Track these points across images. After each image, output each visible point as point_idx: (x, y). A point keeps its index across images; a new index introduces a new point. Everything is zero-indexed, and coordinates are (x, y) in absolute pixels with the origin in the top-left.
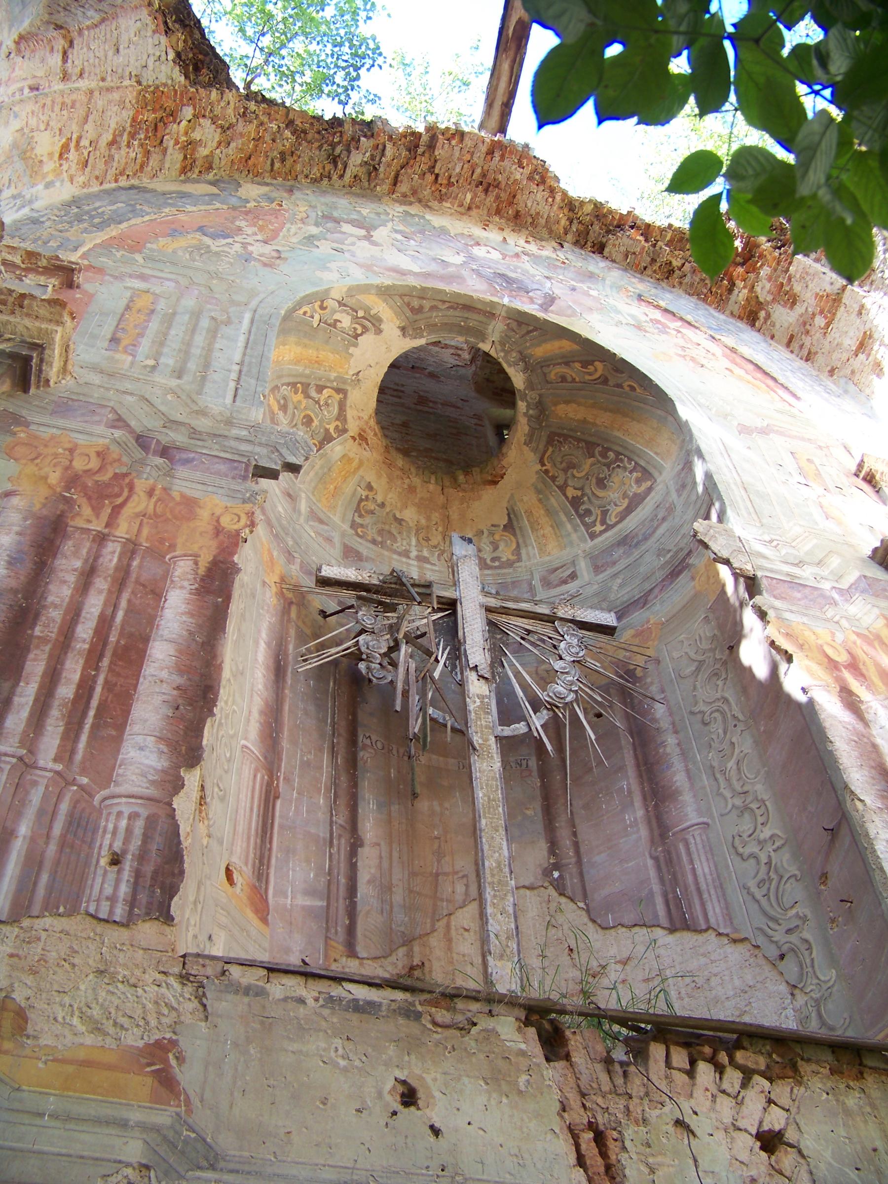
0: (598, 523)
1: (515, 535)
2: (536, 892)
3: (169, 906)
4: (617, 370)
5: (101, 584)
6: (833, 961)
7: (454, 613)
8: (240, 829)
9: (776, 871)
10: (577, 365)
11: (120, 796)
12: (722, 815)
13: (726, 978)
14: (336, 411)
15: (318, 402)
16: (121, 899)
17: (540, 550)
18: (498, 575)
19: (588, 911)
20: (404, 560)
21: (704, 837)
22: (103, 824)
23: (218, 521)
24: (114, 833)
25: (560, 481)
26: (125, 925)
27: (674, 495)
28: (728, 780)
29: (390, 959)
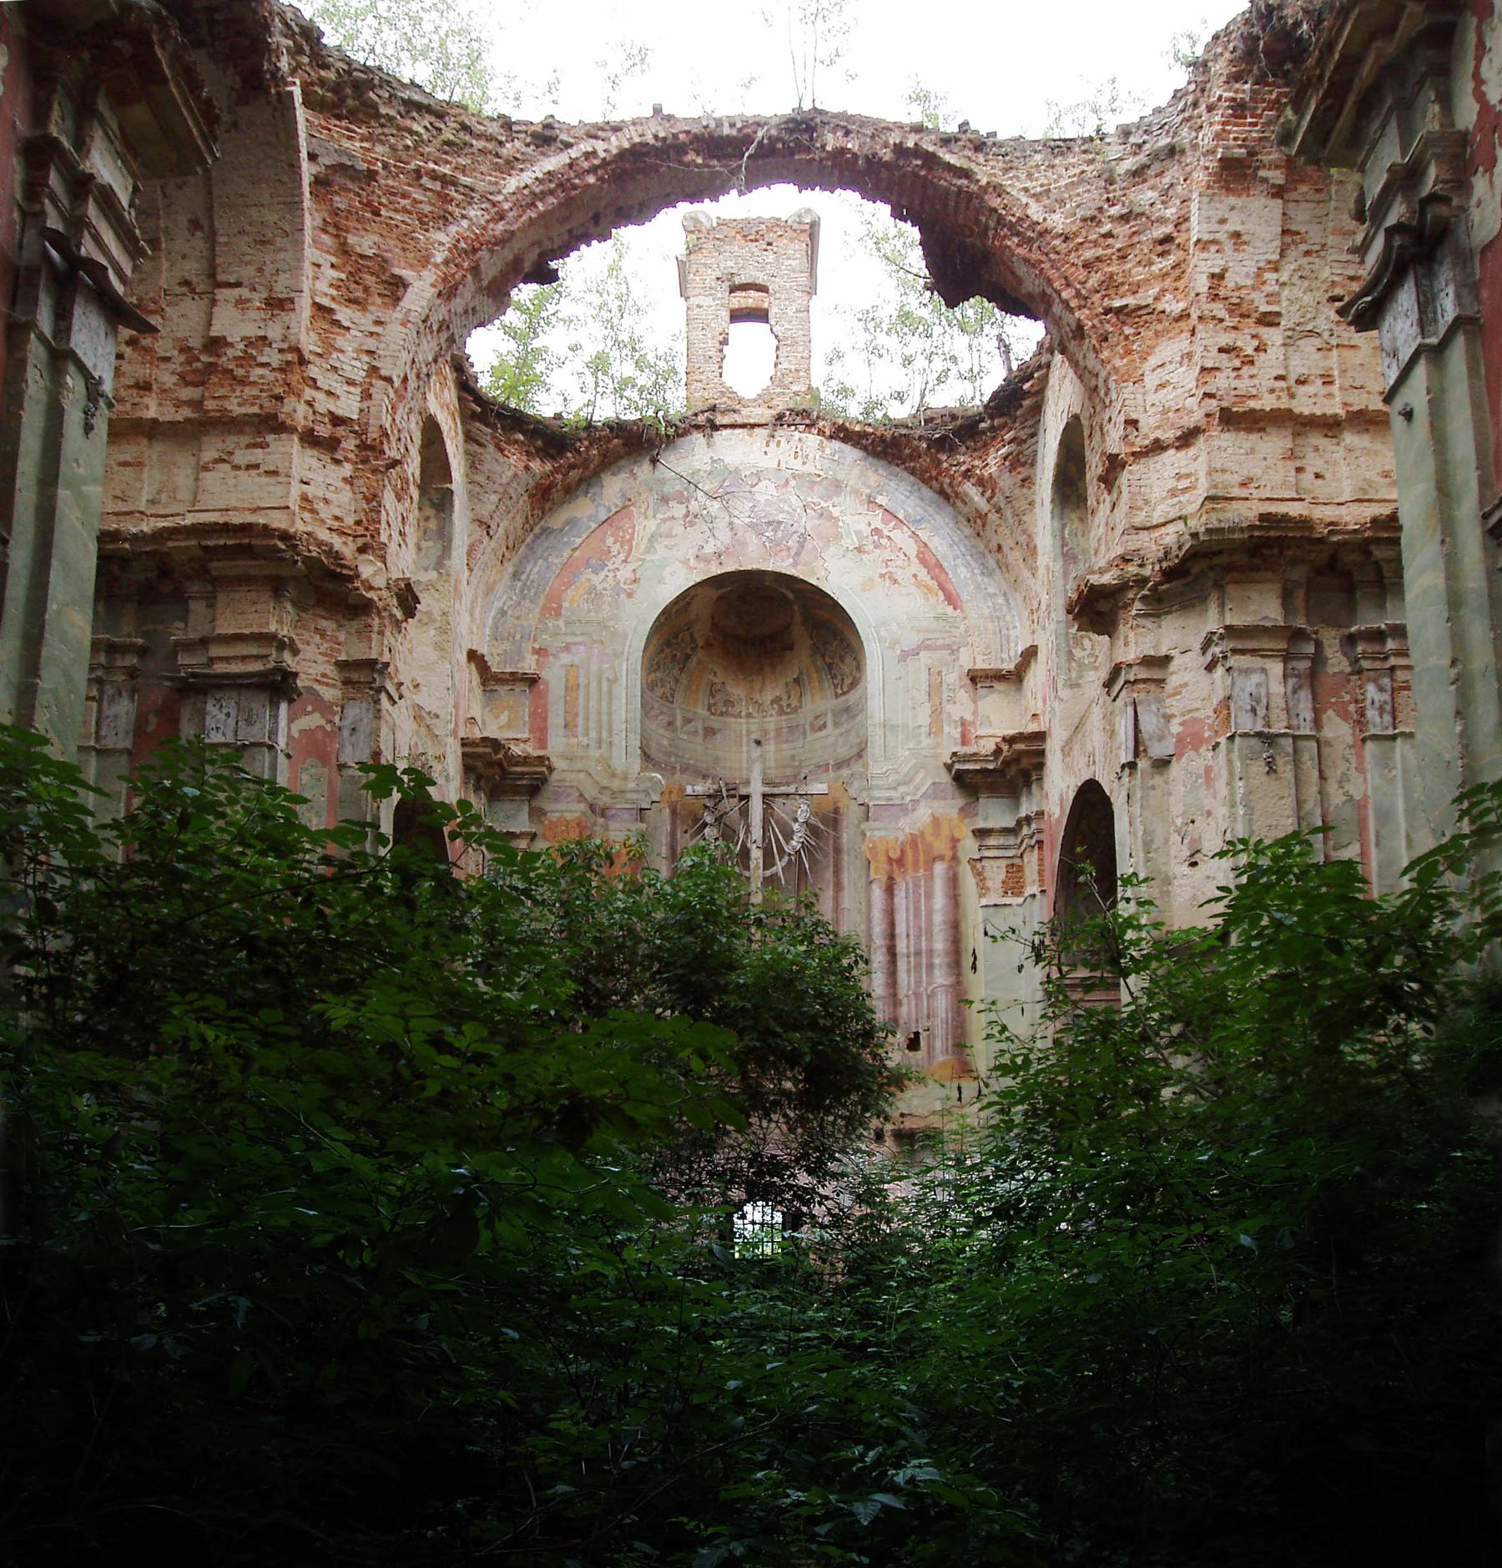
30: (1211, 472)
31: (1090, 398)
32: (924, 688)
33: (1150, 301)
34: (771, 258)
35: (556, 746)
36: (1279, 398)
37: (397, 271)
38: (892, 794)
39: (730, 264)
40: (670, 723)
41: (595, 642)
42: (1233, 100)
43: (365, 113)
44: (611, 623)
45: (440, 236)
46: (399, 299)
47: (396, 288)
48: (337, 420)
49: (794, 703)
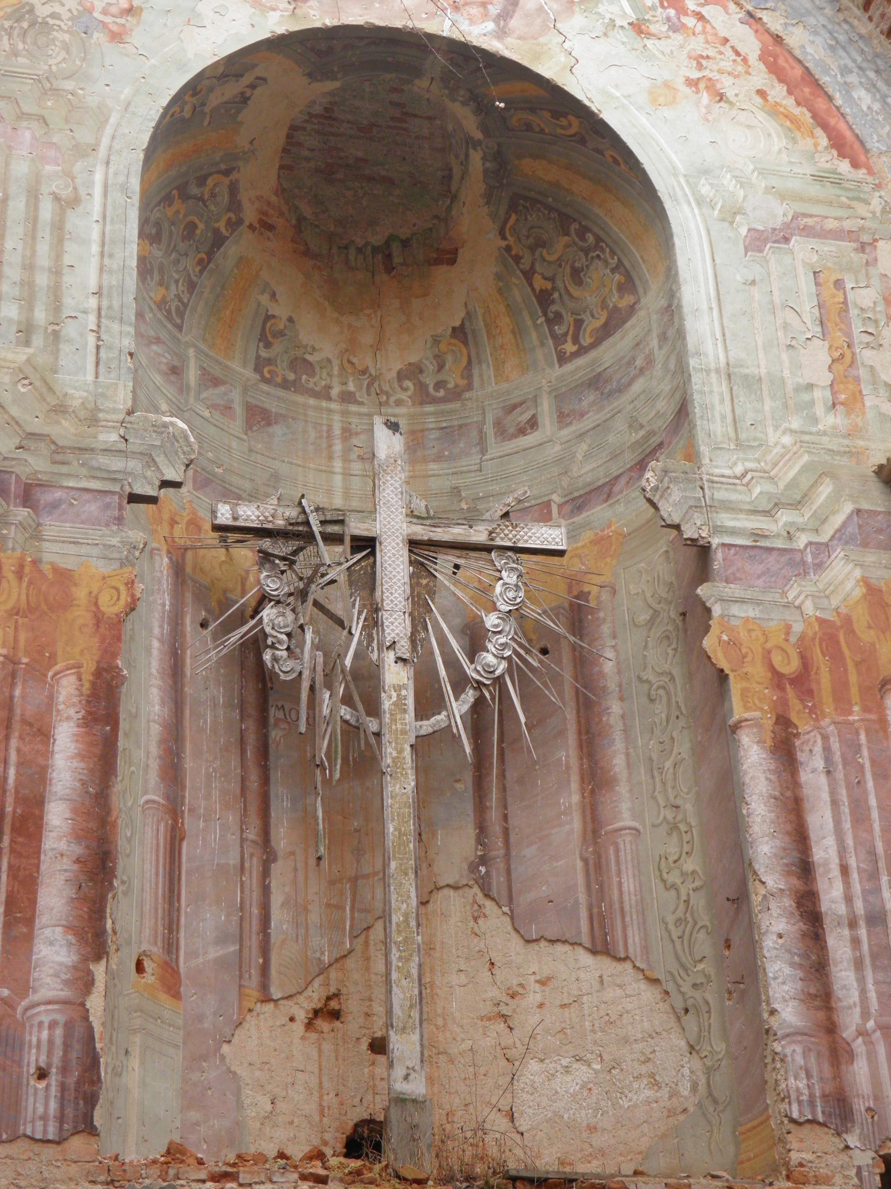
0: (569, 338)
1: (465, 343)
2: (460, 892)
3: (92, 1117)
4: (597, 132)
6: (725, 1036)
7: (373, 553)
8: (147, 908)
9: (692, 915)
10: (547, 115)
11: (38, 1005)
12: (653, 826)
13: (637, 1018)
14: (226, 199)
15: (201, 199)
16: (51, 1117)
17: (497, 369)
18: (442, 413)
19: (512, 918)
20: (324, 404)
21: (634, 848)
22: (28, 1038)
23: (96, 604)
24: (38, 1046)
25: (526, 264)
26: (58, 1143)
27: (654, 343)
28: (664, 783)
29: (305, 994)
32: (808, 307)
41: (23, 116)
49: (454, 380)
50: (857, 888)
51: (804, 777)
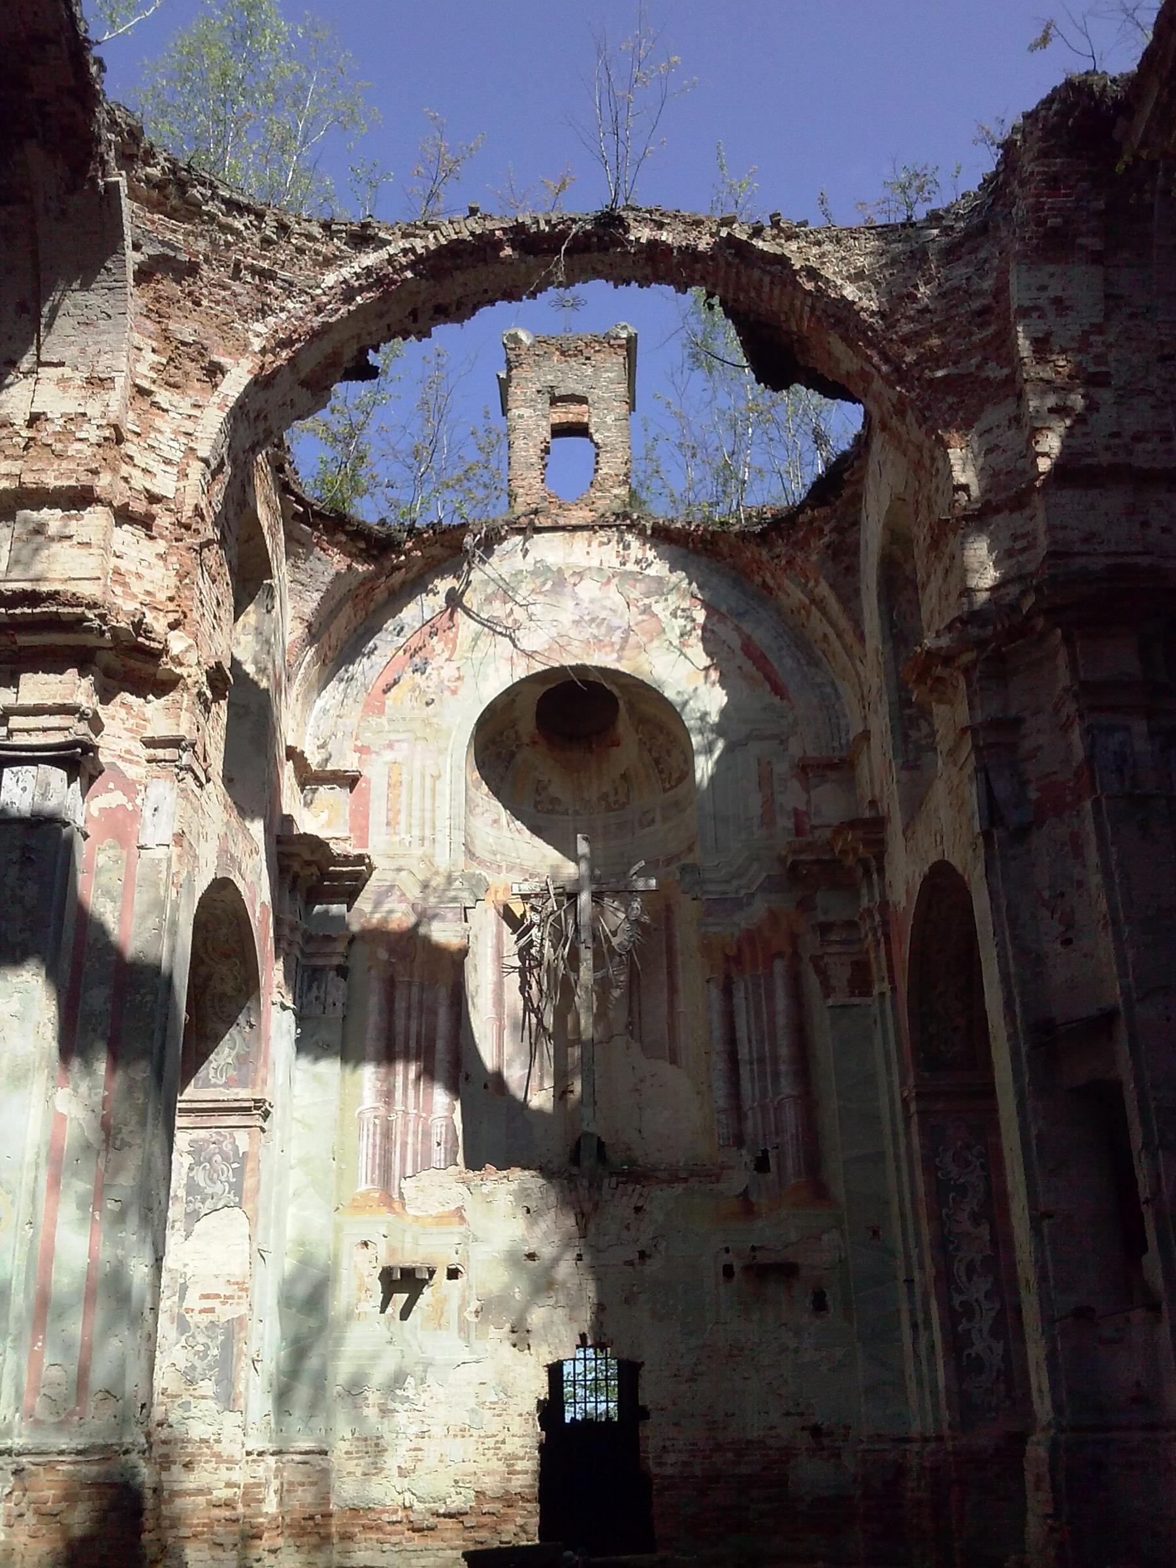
5: (414, 1014)
30: (1051, 528)
31: (915, 472)
33: (973, 369)
34: (590, 371)
35: (377, 848)
36: (1115, 454)
37: (216, 358)
38: (723, 887)
39: (549, 377)
40: (495, 821)
42: (1044, 173)
43: (190, 211)
44: (434, 720)
45: (258, 327)
46: (216, 386)
47: (214, 371)
48: (153, 499)
50: (754, 1048)
51: (735, 1001)
